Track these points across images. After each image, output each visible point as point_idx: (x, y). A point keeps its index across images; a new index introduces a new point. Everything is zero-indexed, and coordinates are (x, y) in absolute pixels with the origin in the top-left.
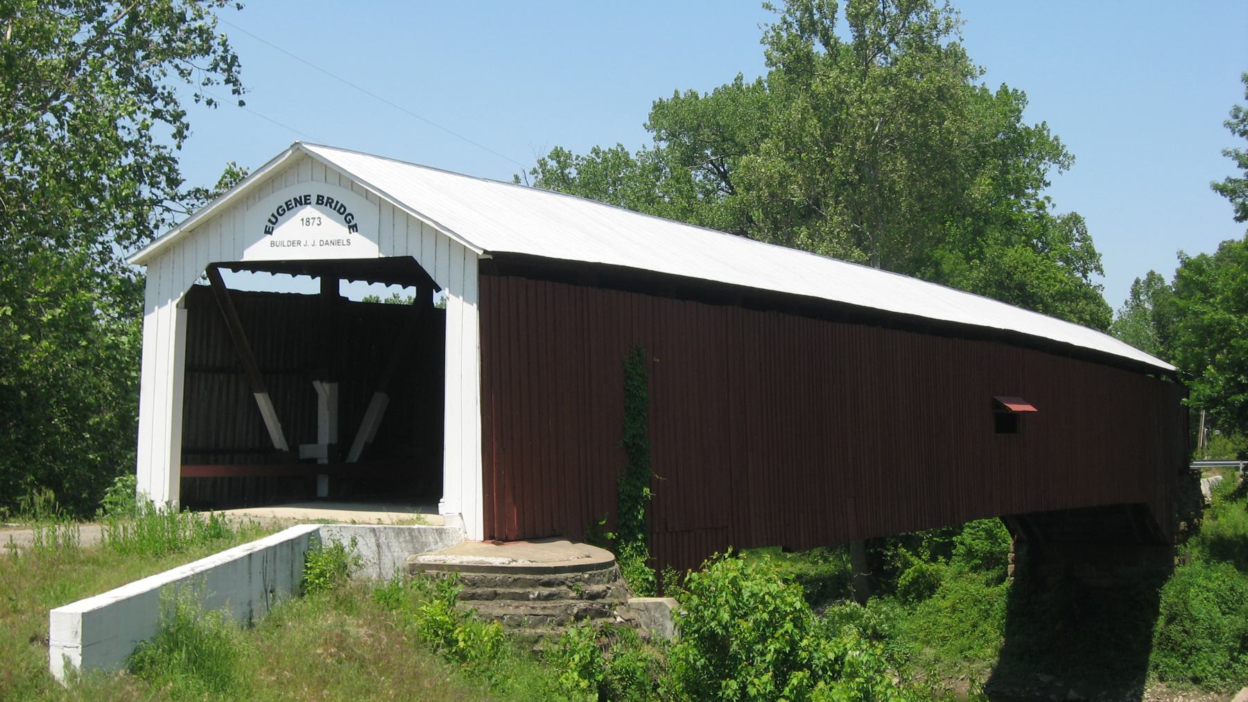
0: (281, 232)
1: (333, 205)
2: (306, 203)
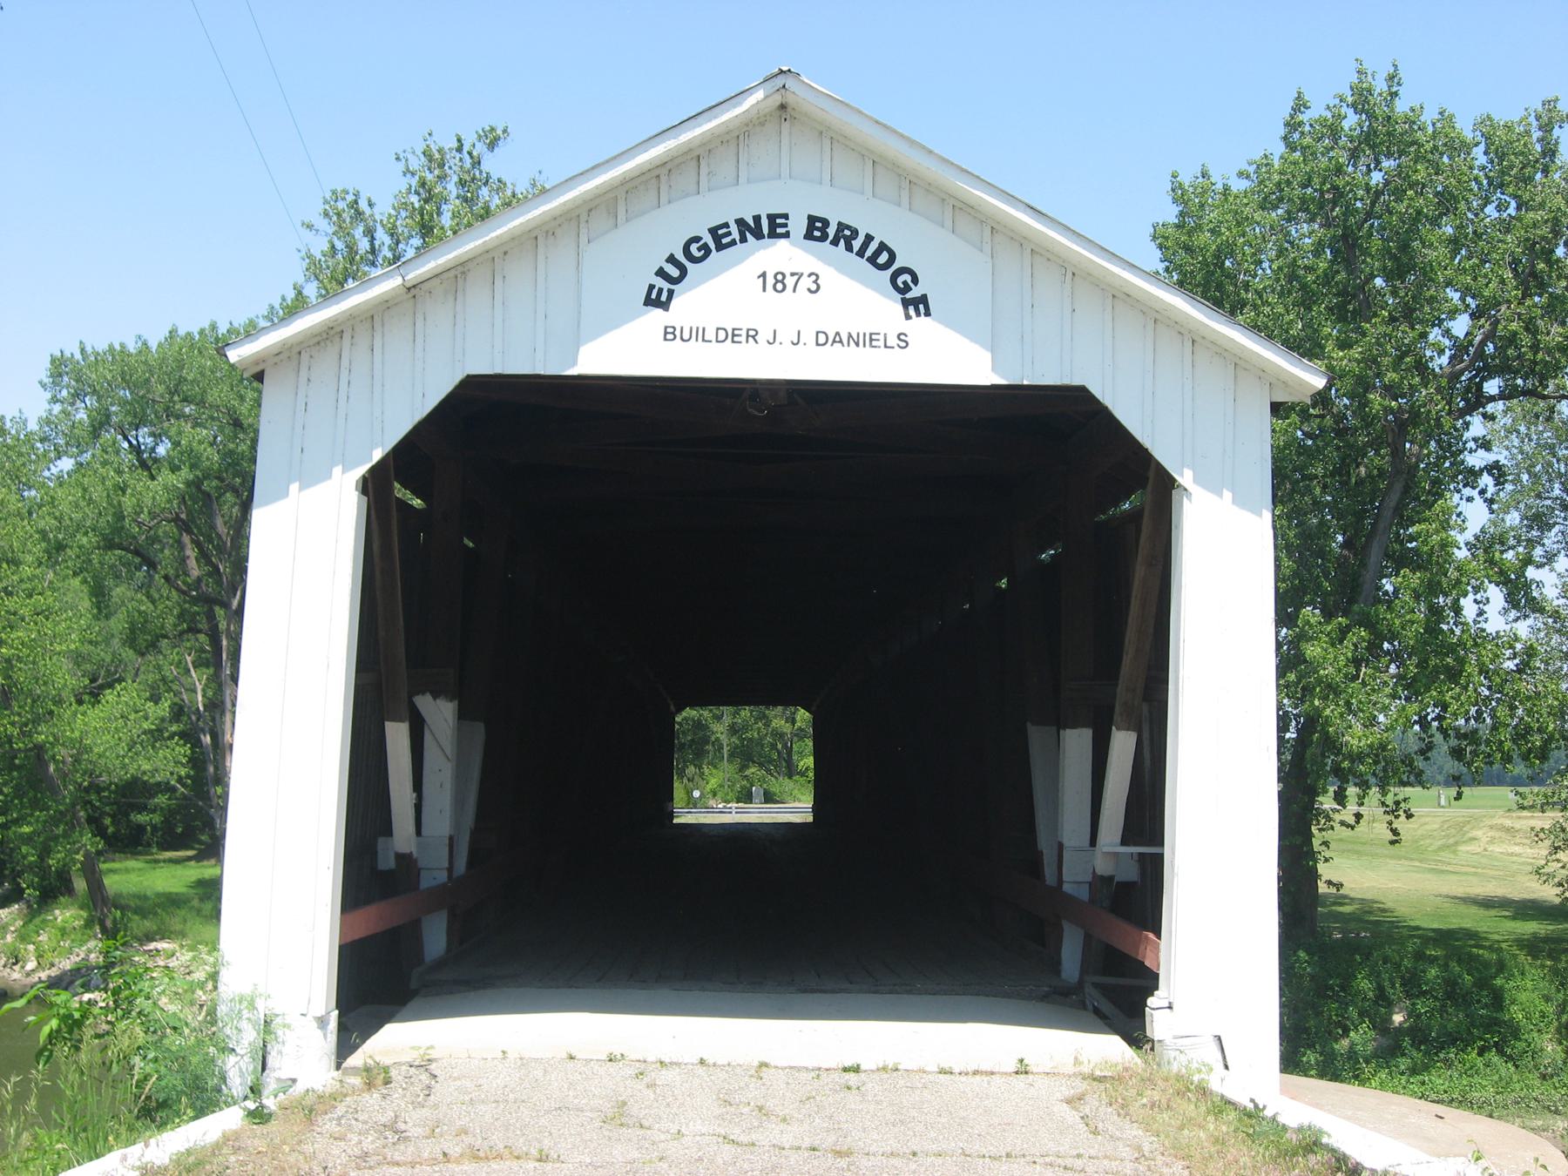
0: (689, 305)
1: (857, 244)
2: (773, 234)
